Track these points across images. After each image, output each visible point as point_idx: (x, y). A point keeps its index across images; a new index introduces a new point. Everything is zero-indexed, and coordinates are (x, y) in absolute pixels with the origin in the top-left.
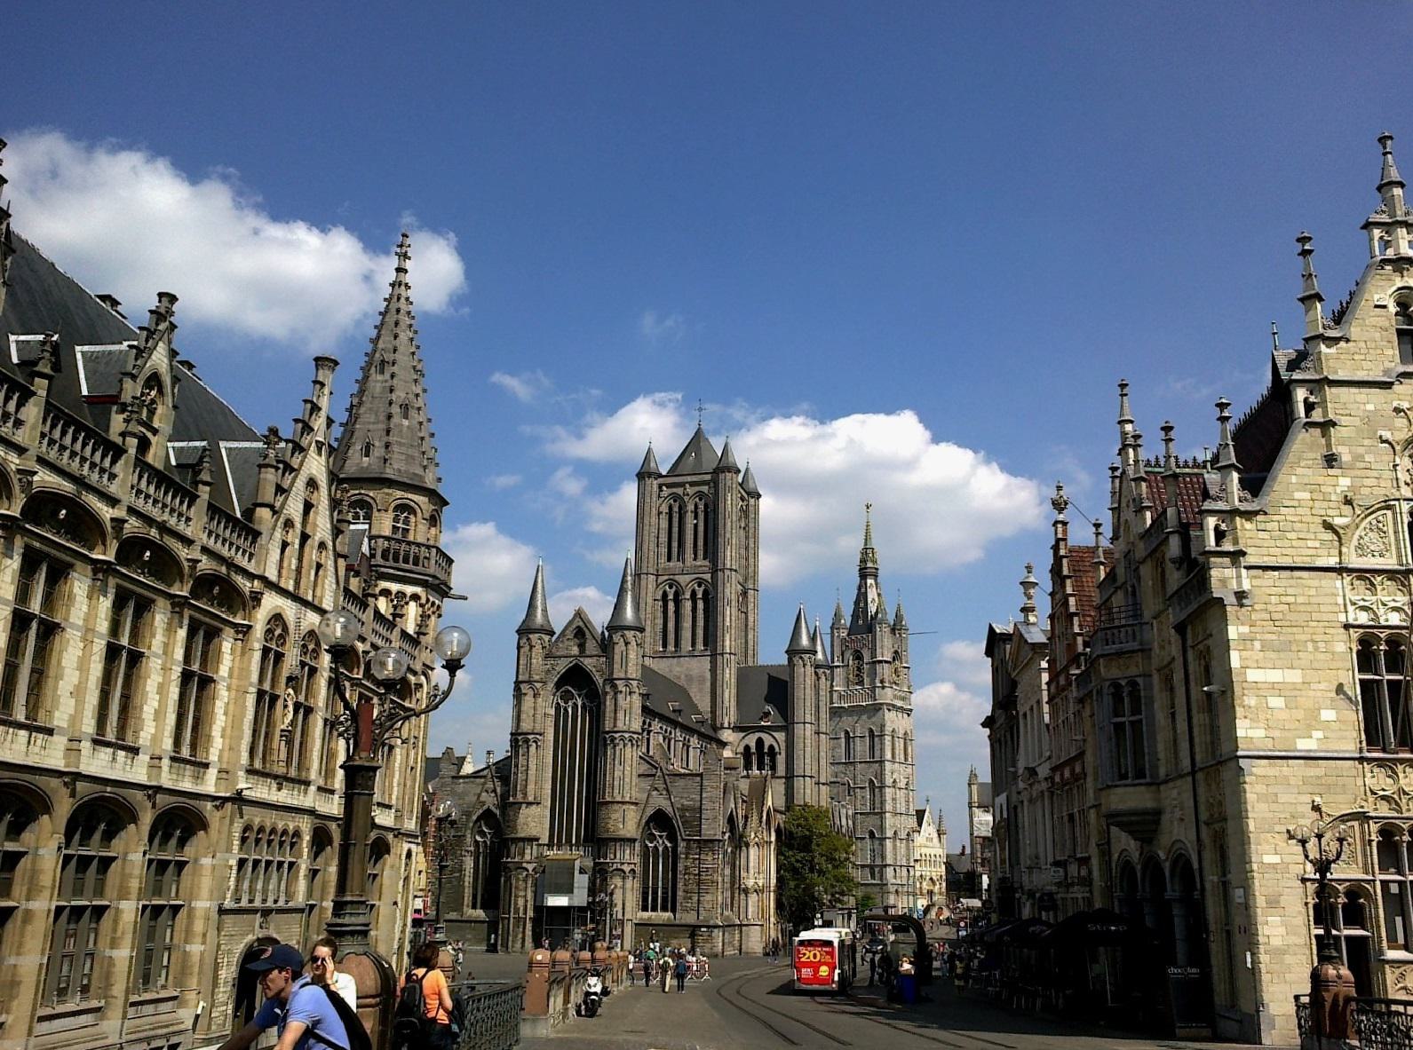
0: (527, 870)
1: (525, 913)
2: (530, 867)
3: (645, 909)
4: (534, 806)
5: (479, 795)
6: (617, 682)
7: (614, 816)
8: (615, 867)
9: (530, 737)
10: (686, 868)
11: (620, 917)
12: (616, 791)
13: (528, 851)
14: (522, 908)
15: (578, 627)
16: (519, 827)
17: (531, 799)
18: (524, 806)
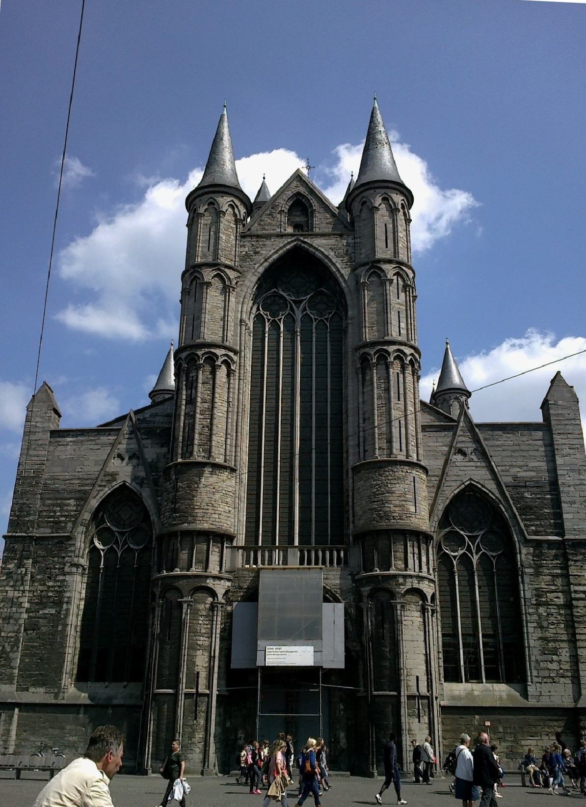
0: (213, 594)
1: (209, 686)
2: (220, 588)
3: (452, 675)
4: (225, 474)
5: (106, 462)
6: (385, 267)
7: (399, 488)
8: (408, 586)
9: (219, 352)
10: (539, 593)
11: (423, 690)
12: (396, 445)
13: (214, 558)
14: (203, 675)
15: (298, 194)
16: (199, 512)
17: (220, 460)
18: (208, 470)
